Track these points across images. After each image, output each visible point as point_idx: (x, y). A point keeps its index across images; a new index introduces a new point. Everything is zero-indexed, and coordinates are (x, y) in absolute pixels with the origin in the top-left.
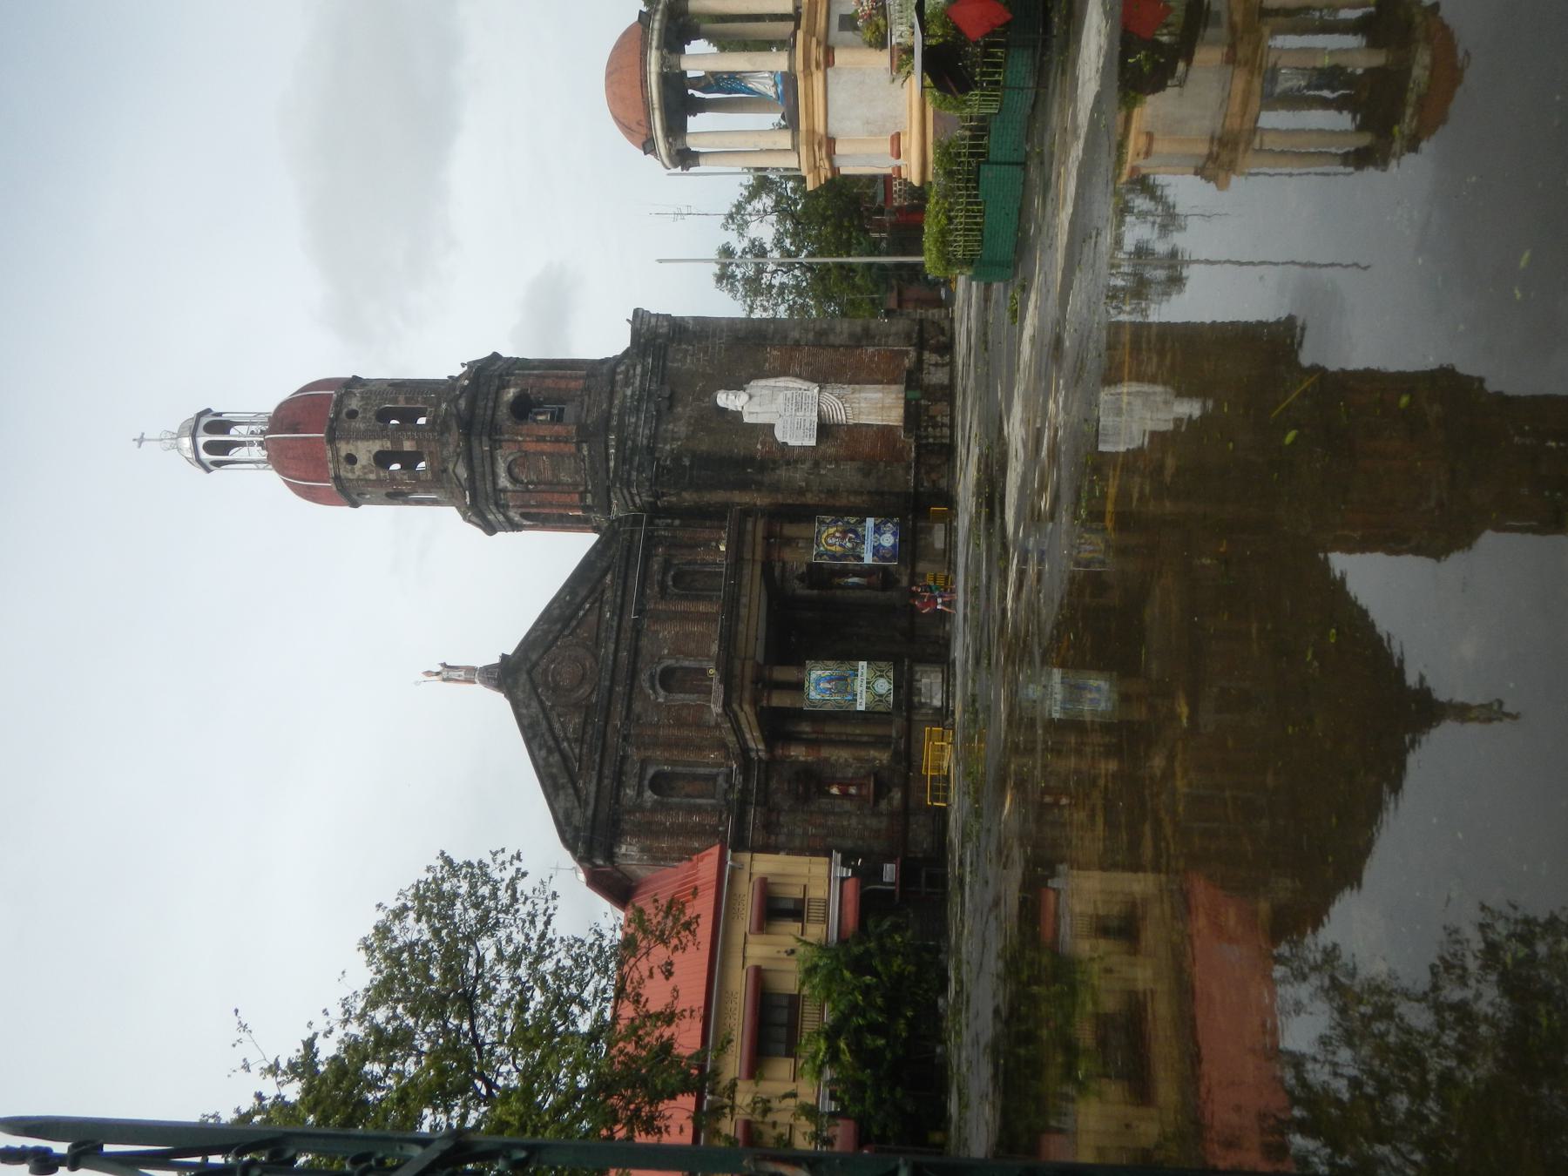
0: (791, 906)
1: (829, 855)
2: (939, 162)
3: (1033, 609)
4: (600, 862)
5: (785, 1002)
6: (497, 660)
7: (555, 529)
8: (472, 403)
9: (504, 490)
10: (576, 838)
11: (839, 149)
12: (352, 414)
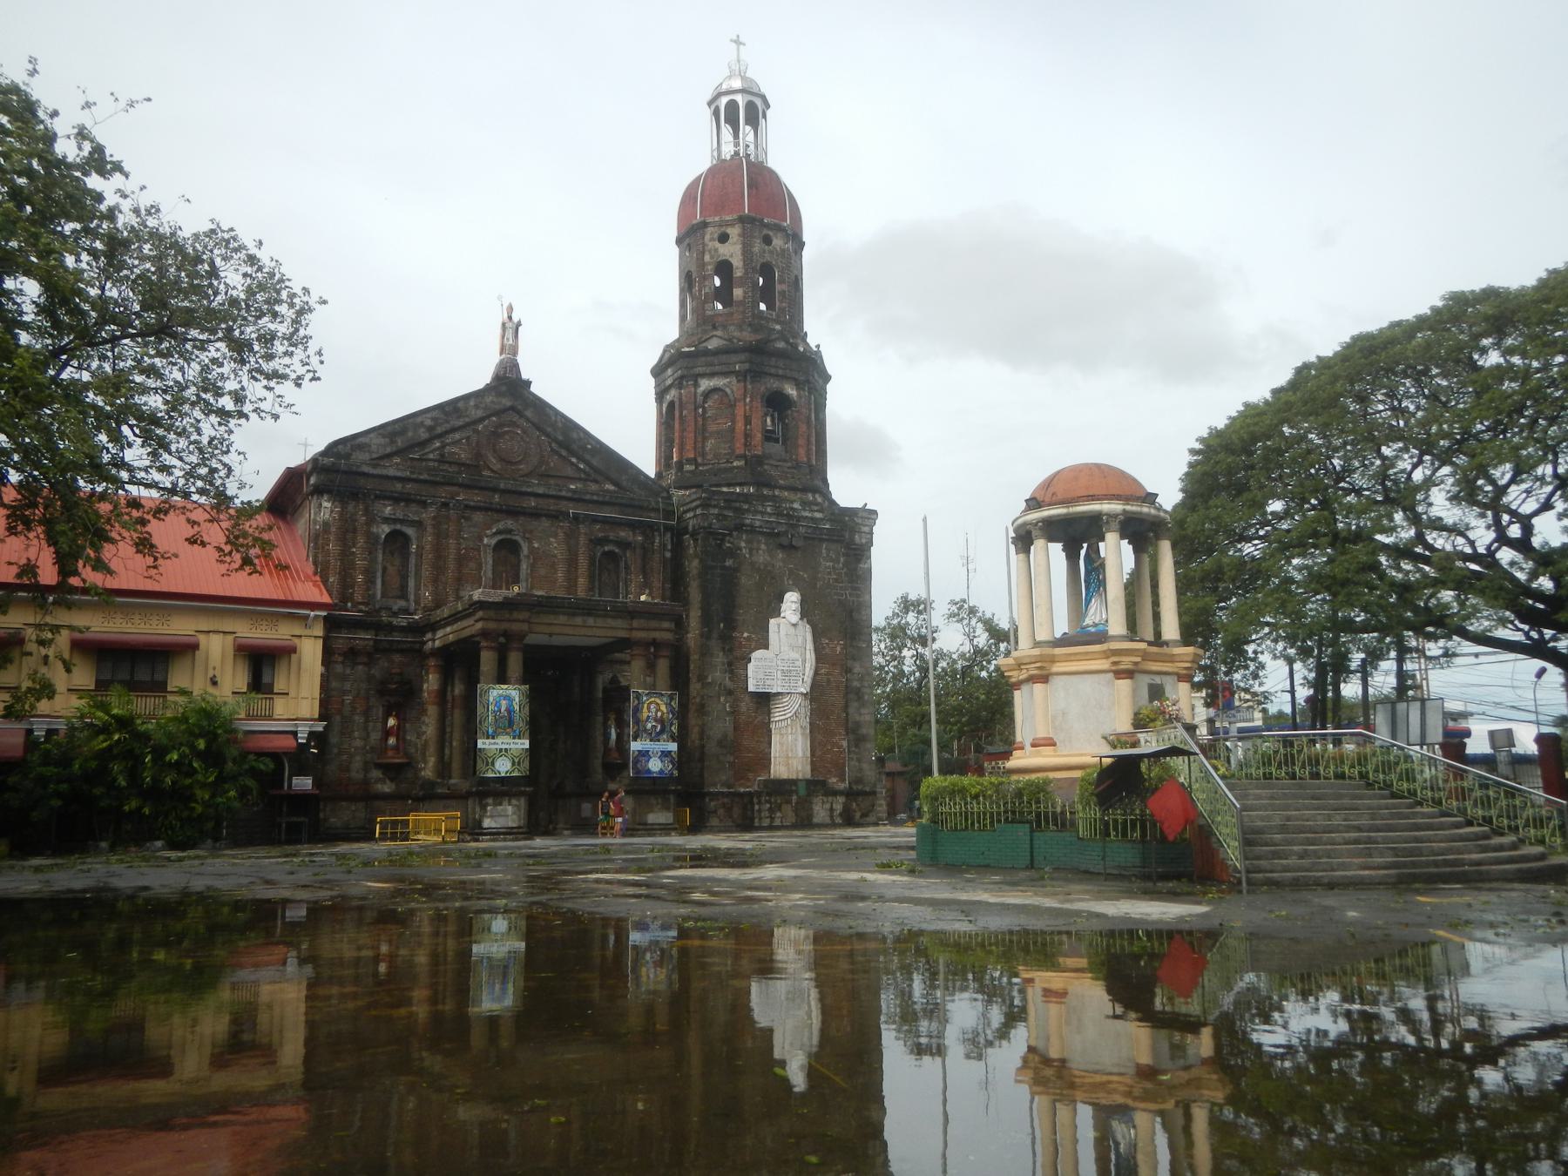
0: (266, 679)
1: (321, 719)
2: (1030, 784)
3: (585, 894)
4: (312, 481)
5: (158, 677)
6: (524, 376)
7: (659, 435)
8: (781, 354)
9: (696, 385)
10: (338, 456)
11: (1038, 687)
12: (767, 240)
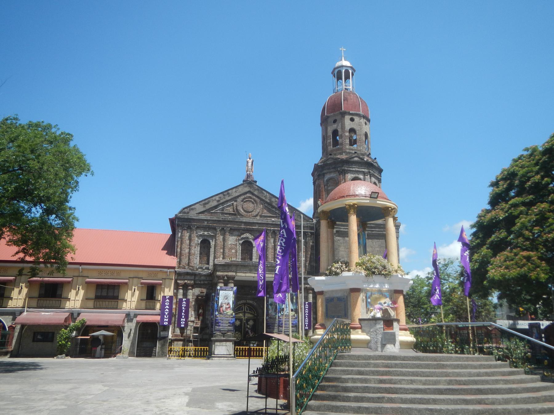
5: (115, 295)
8: (356, 163)
10: (185, 213)
12: (352, 120)
